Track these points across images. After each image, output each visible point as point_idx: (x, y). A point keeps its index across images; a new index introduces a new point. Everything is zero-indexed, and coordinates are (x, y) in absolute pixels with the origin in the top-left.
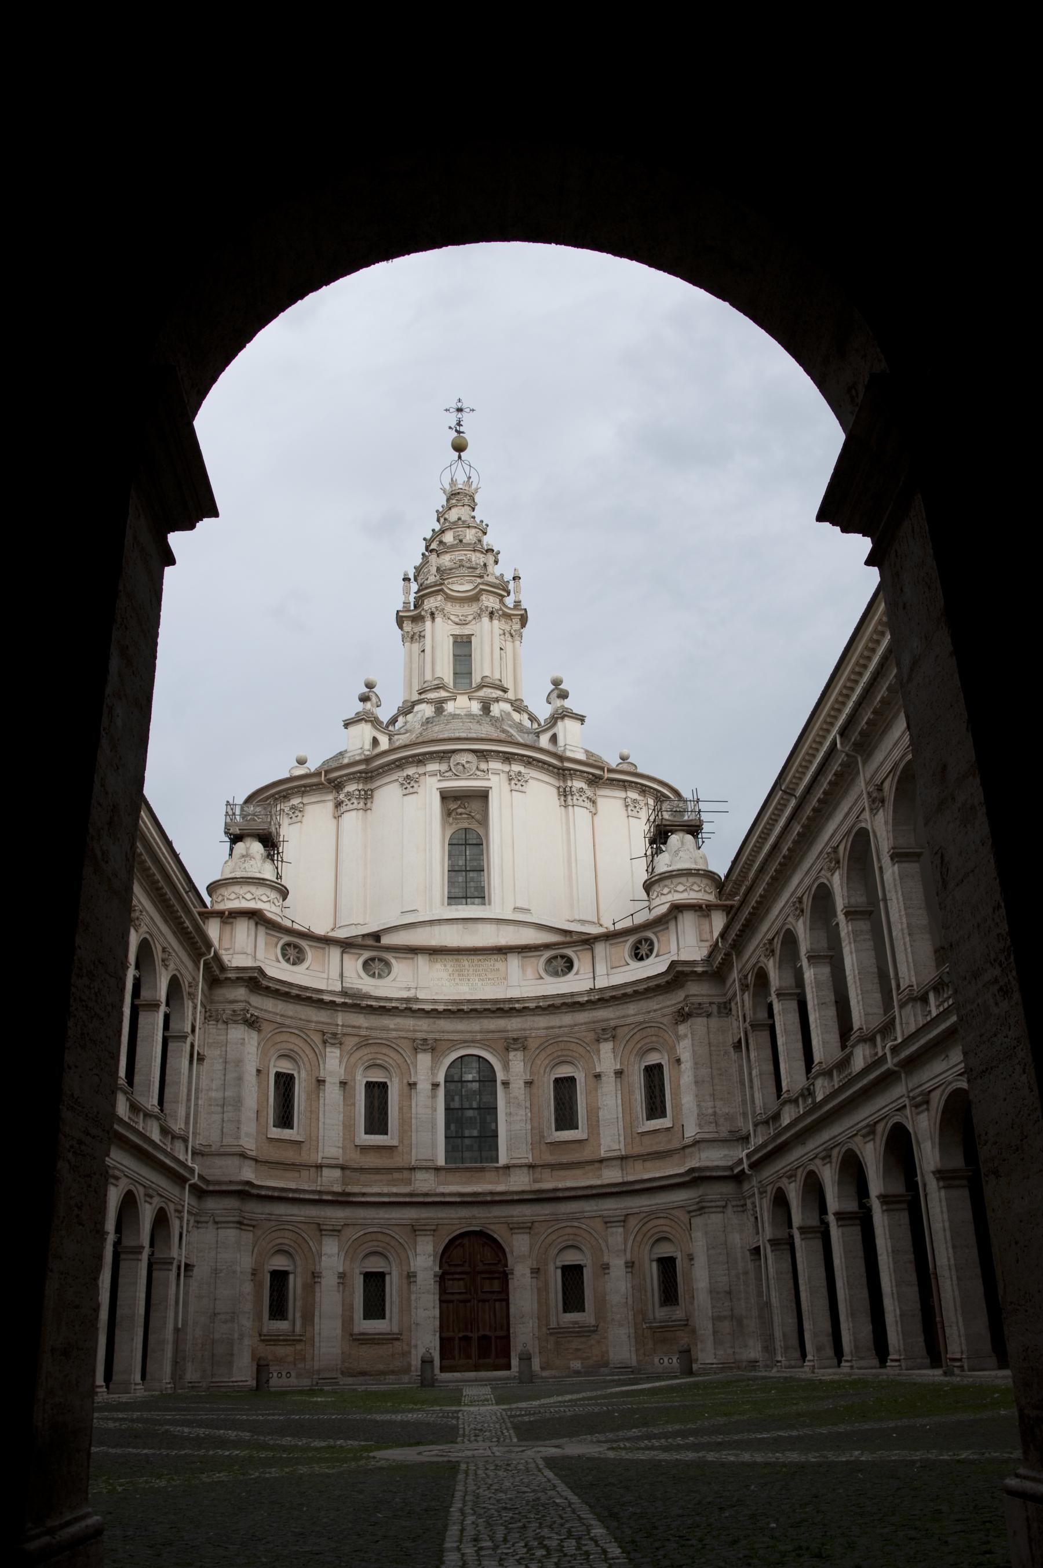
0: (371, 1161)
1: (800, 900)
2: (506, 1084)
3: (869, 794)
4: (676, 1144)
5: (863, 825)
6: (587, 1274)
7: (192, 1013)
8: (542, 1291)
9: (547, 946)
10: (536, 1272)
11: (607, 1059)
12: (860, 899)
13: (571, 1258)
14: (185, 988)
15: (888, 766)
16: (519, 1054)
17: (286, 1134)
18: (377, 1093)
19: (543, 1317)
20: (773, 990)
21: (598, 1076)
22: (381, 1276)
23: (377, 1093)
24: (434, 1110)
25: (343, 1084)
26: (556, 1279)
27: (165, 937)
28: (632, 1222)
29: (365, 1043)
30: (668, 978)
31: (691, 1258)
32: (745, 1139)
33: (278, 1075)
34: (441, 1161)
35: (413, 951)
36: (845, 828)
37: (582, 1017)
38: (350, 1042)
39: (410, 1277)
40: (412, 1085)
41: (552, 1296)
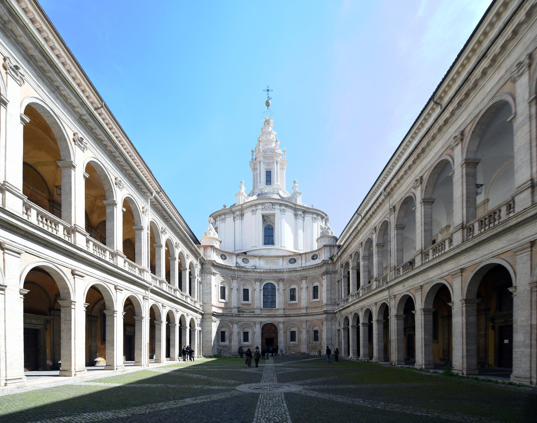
0: (245, 307)
1: (362, 243)
2: (278, 290)
3: (390, 209)
4: (320, 305)
5: (386, 219)
6: (297, 333)
7: (197, 271)
8: (285, 337)
9: (290, 256)
10: (285, 332)
11: (304, 284)
12: (381, 241)
13: (293, 329)
14: (195, 266)
15: (398, 200)
16: (282, 283)
17: (223, 300)
18: (246, 292)
19: (286, 342)
20: (350, 268)
21: (302, 288)
22: (248, 332)
23: (246, 292)
24: (260, 295)
25: (237, 289)
26: (289, 334)
27: (186, 252)
28: (308, 322)
29: (243, 279)
30: (321, 264)
31: (322, 331)
32: (338, 305)
33: (221, 287)
34: (262, 307)
35: (256, 256)
36: (380, 221)
37: (298, 274)
38: (239, 279)
39: (254, 333)
40: (255, 290)
41: (288, 338)
